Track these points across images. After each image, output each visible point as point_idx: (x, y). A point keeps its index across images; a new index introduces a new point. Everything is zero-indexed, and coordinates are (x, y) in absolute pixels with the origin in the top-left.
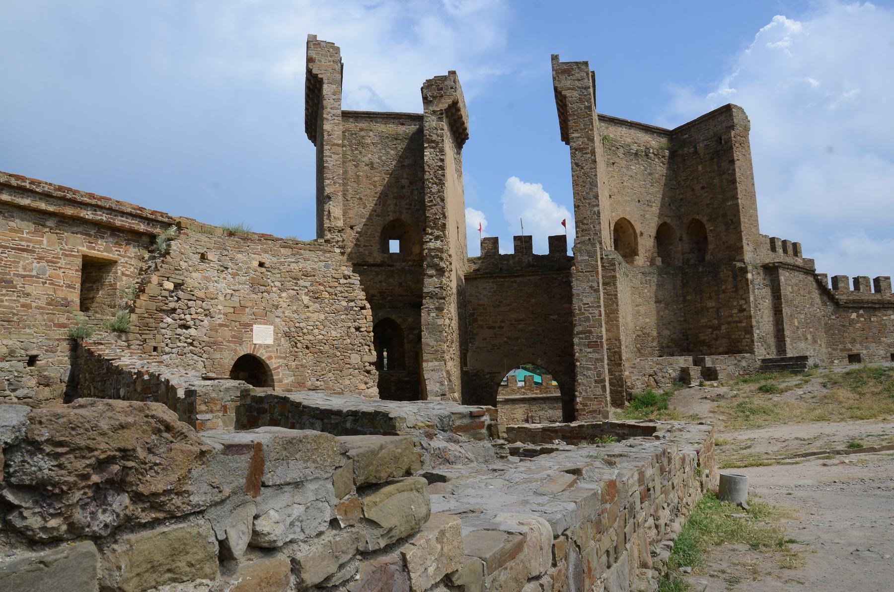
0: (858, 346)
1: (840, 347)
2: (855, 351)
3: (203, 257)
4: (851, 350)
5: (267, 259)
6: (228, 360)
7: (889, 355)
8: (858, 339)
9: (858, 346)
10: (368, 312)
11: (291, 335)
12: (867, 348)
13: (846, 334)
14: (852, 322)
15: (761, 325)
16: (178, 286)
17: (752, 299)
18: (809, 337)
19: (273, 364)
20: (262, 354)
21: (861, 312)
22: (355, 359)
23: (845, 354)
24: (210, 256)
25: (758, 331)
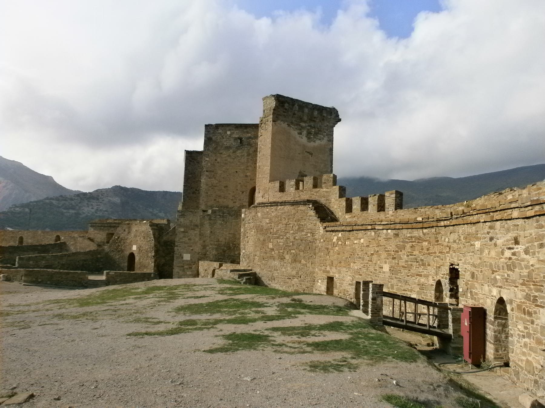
0: (334, 270)
1: (323, 268)
2: (331, 275)
3: (125, 230)
4: (328, 272)
5: (137, 229)
6: (127, 253)
7: (354, 282)
8: (335, 262)
9: (334, 270)
10: (153, 241)
11: (139, 248)
12: (340, 272)
13: (328, 257)
14: (334, 245)
15: (247, 247)
16: (119, 238)
17: (242, 230)
18: (287, 257)
19: (136, 255)
20: (134, 253)
21: (340, 235)
22: (150, 254)
23: (325, 276)
24: (126, 230)
25: (244, 251)
